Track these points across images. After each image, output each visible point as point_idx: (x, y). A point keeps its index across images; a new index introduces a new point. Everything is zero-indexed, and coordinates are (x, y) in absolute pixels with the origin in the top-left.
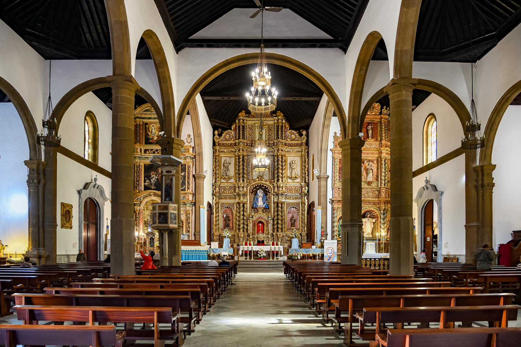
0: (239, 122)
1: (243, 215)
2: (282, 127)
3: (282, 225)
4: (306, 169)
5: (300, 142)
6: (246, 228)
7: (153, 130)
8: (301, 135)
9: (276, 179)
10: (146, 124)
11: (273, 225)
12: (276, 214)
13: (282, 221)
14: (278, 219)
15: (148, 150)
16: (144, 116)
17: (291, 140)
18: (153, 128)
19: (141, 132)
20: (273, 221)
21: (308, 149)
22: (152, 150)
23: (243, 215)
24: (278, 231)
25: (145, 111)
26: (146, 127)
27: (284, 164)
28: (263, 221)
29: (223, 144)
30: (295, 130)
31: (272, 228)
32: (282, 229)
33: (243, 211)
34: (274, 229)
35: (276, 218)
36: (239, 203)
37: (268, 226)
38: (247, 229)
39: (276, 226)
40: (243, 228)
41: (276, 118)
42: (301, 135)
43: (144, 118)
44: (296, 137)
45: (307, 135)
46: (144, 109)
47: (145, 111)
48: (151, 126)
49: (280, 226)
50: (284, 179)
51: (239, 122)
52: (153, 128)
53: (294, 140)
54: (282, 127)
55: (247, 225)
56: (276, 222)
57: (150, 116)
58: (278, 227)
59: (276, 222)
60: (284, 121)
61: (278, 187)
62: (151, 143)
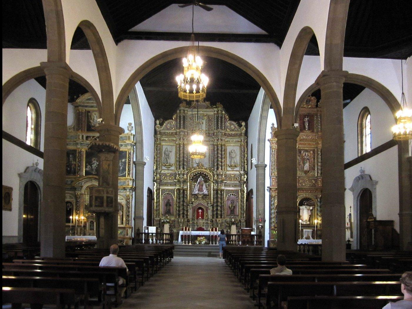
0: (180, 113)
1: (183, 201)
2: (222, 118)
3: (221, 211)
4: (245, 158)
5: (239, 133)
6: (186, 214)
8: (240, 126)
9: (216, 167)
10: (89, 112)
11: (213, 211)
12: (215, 200)
13: (221, 207)
14: (217, 206)
17: (230, 131)
20: (213, 208)
21: (247, 139)
22: (93, 137)
23: (183, 201)
24: (217, 217)
26: (88, 115)
27: (223, 153)
28: (203, 207)
29: (165, 133)
30: (235, 121)
31: (211, 214)
32: (221, 215)
33: (183, 197)
34: (213, 215)
35: (215, 205)
36: (179, 190)
37: (207, 212)
38: (187, 215)
39: (215, 213)
40: (183, 213)
41: (216, 109)
42: (240, 126)
44: (235, 127)
45: (247, 126)
48: (93, 114)
49: (219, 212)
50: (223, 168)
51: (180, 113)
53: (233, 130)
54: (222, 118)
55: (187, 211)
56: (215, 208)
58: (217, 214)
59: (215, 208)
60: (224, 112)
61: (217, 175)
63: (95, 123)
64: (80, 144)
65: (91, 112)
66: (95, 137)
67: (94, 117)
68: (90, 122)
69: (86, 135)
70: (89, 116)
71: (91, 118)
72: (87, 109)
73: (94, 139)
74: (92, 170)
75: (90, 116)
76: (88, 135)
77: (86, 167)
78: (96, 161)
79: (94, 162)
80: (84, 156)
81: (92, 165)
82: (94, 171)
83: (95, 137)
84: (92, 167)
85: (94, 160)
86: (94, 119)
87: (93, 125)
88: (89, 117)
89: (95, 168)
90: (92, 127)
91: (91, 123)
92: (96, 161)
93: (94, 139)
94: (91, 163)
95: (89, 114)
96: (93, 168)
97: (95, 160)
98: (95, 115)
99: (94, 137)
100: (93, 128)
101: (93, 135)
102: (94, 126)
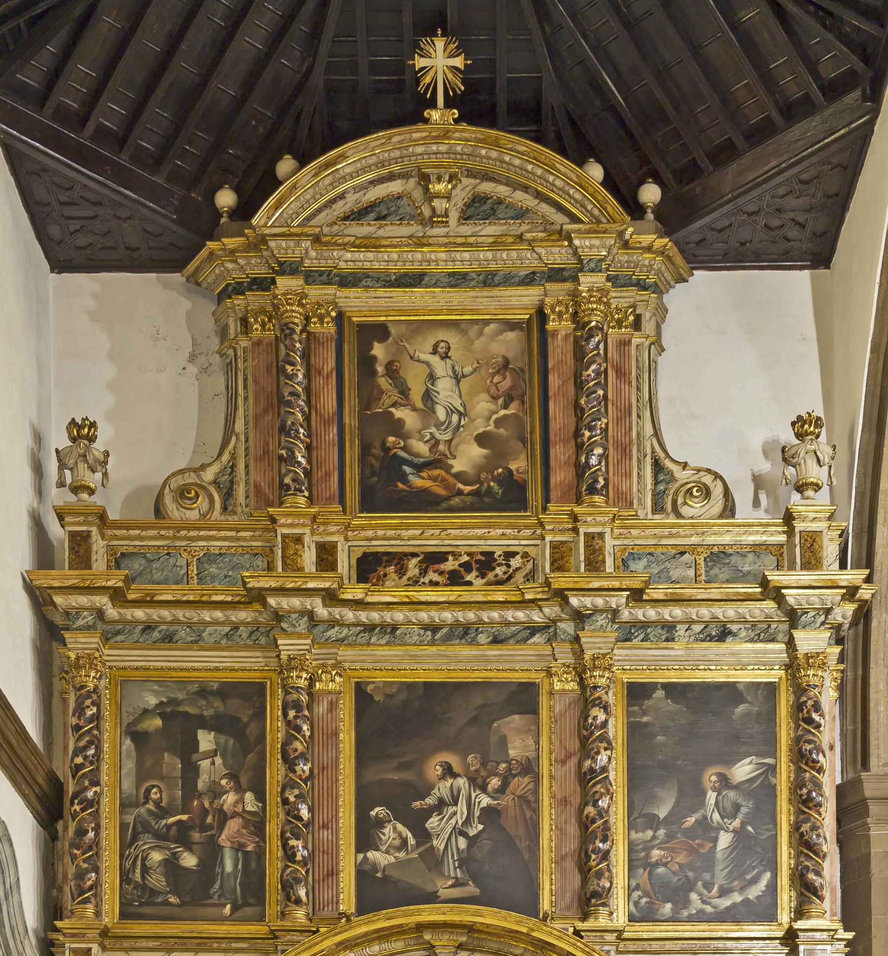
7: (444, 388)
10: (380, 331)
15: (399, 560)
16: (348, 260)
18: (440, 367)
19: (328, 401)
22: (433, 559)
25: (359, 215)
26: (367, 363)
43: (348, 280)
46: (351, 202)
47: (359, 215)
48: (422, 349)
52: (440, 367)
57: (413, 260)
62: (423, 502)
63: (443, 437)
64: (303, 625)
65: (393, 330)
66: (451, 565)
67: (432, 378)
68: (397, 428)
69: (361, 547)
70: (380, 369)
71: (404, 392)
72: (359, 303)
73: (435, 577)
74: (433, 861)
75: (392, 371)
76: (379, 546)
77: (366, 838)
78: (462, 782)
79: (443, 788)
80: (347, 739)
81: (428, 813)
82: (451, 867)
83: (451, 565)
84: (423, 836)
85: (449, 772)
86: (428, 397)
87: (422, 448)
88: (383, 382)
89: (462, 843)
90: (419, 468)
91: (405, 437)
92: (462, 782)
93: (435, 577)
94: (417, 804)
95: (378, 350)
96: (439, 844)
97: (456, 768)
98: (445, 356)
99: (441, 557)
100: (417, 482)
101: (432, 544)
102: (438, 462)
